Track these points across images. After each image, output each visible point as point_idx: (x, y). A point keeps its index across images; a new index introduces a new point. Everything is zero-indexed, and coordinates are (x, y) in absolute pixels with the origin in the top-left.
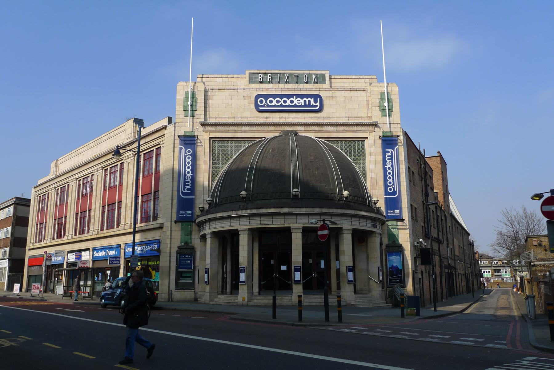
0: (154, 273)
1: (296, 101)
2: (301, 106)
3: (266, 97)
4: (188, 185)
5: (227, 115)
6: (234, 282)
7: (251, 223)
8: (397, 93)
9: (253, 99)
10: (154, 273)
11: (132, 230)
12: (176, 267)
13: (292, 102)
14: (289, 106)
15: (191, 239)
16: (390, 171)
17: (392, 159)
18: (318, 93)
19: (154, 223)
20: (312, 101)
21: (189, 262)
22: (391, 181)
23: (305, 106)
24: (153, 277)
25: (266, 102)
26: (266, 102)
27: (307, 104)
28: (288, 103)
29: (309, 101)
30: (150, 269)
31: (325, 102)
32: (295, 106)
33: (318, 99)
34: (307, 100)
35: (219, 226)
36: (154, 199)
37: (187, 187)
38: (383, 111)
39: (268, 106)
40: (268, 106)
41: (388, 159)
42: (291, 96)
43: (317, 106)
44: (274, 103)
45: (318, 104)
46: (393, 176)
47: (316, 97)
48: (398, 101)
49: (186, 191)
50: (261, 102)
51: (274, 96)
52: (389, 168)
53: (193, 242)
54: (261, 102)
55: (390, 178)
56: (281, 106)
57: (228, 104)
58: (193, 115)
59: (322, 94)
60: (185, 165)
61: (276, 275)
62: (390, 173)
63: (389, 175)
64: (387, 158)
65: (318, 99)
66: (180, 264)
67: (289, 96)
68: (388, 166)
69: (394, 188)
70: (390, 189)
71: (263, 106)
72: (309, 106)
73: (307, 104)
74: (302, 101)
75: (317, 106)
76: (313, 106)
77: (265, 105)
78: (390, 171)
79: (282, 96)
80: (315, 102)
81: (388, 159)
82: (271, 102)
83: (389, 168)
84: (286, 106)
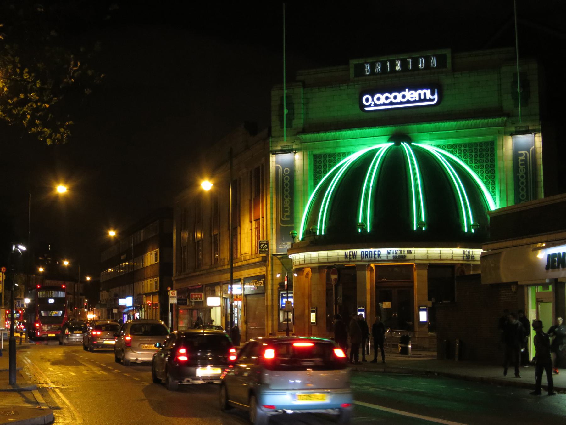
2: (415, 101)
11: (229, 267)
23: (420, 100)
25: (373, 100)
26: (373, 100)
28: (399, 99)
29: (425, 94)
32: (408, 102)
37: (287, 214)
38: (515, 98)
39: (376, 105)
40: (376, 105)
43: (433, 100)
44: (383, 100)
46: (526, 186)
49: (285, 219)
50: (367, 100)
56: (391, 103)
63: (522, 186)
71: (370, 106)
72: (425, 100)
73: (422, 97)
75: (433, 100)
76: (431, 100)
82: (379, 99)
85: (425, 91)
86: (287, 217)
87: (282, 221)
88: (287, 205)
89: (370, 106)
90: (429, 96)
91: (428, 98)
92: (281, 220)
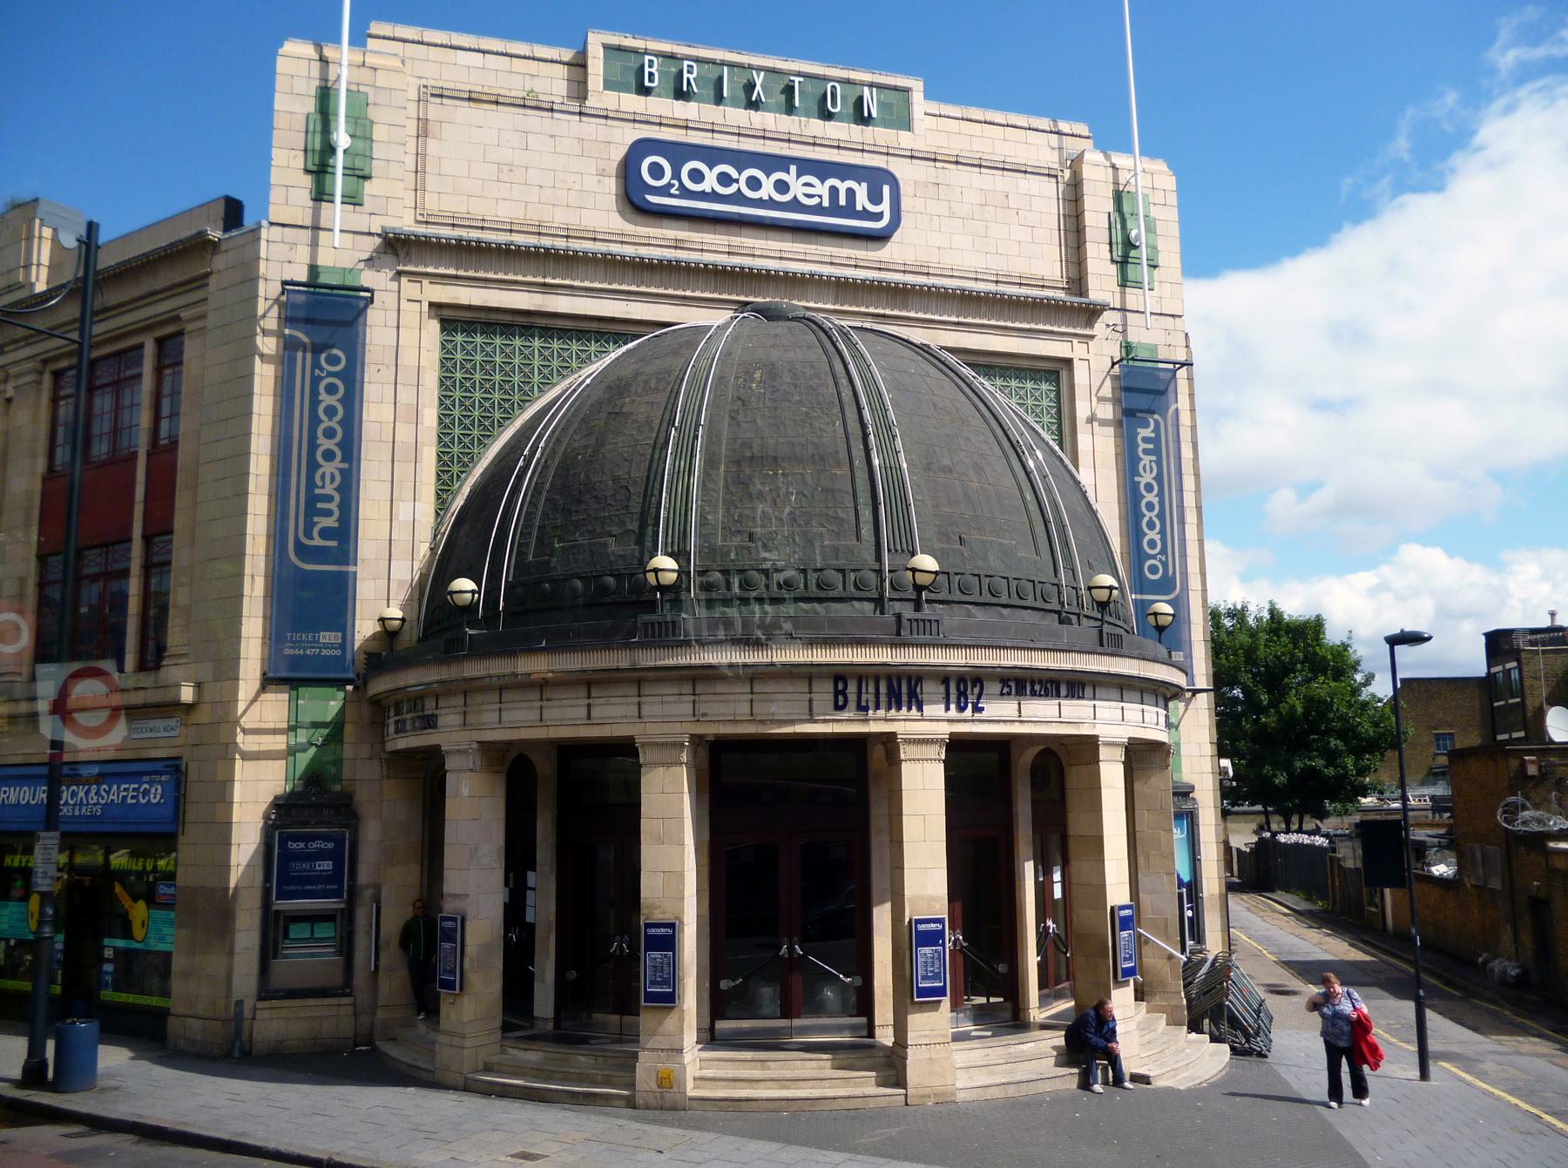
0: (139, 911)
1: (798, 187)
2: (818, 210)
3: (678, 153)
4: (328, 513)
5: (504, 212)
6: (572, 975)
7: (701, 708)
8: (1173, 199)
9: (619, 153)
10: (139, 911)
12: (266, 893)
13: (782, 187)
14: (771, 204)
15: (338, 762)
16: (1151, 497)
17: (1156, 452)
18: (884, 166)
19: (146, 679)
20: (861, 191)
21: (326, 865)
22: (1153, 535)
23: (835, 210)
24: (138, 932)
25: (676, 175)
26: (676, 175)
27: (842, 202)
28: (767, 190)
29: (851, 193)
30: (118, 889)
31: (905, 204)
32: (795, 205)
33: (886, 189)
34: (842, 187)
35: (522, 722)
36: (147, 568)
41: (1146, 452)
42: (782, 163)
43: (879, 216)
44: (710, 183)
45: (885, 207)
46: (1161, 516)
47: (877, 179)
48: (1175, 229)
49: (318, 541)
51: (713, 156)
52: (1149, 488)
53: (347, 772)
54: (656, 171)
55: (1151, 525)
56: (739, 198)
57: (511, 167)
58: (353, 200)
59: (897, 167)
60: (315, 421)
61: (791, 950)
62: (1150, 506)
63: (1148, 515)
64: (1142, 446)
65: (886, 189)
66: (284, 878)
67: (771, 163)
68: (1146, 478)
69: (1165, 565)
70: (1153, 570)
71: (664, 191)
72: (850, 211)
73: (842, 202)
74: (822, 189)
76: (866, 215)
77: (670, 185)
78: (1151, 497)
79: (742, 159)
80: (875, 198)
81: (1146, 452)
82: (697, 176)
83: (1149, 488)
84: (759, 203)
85: (851, 184)
86: (326, 533)
87: (301, 550)
88: (329, 489)
89: (664, 191)
90: (862, 200)
91: (859, 208)
92: (297, 542)
